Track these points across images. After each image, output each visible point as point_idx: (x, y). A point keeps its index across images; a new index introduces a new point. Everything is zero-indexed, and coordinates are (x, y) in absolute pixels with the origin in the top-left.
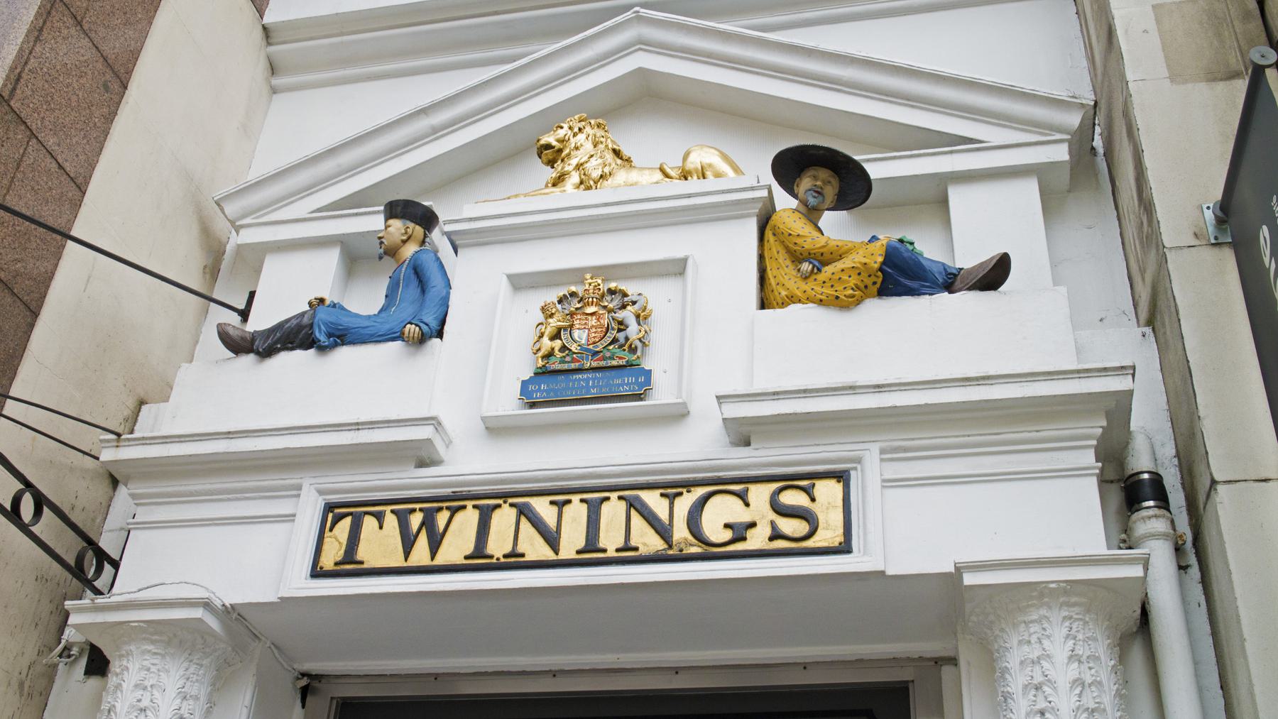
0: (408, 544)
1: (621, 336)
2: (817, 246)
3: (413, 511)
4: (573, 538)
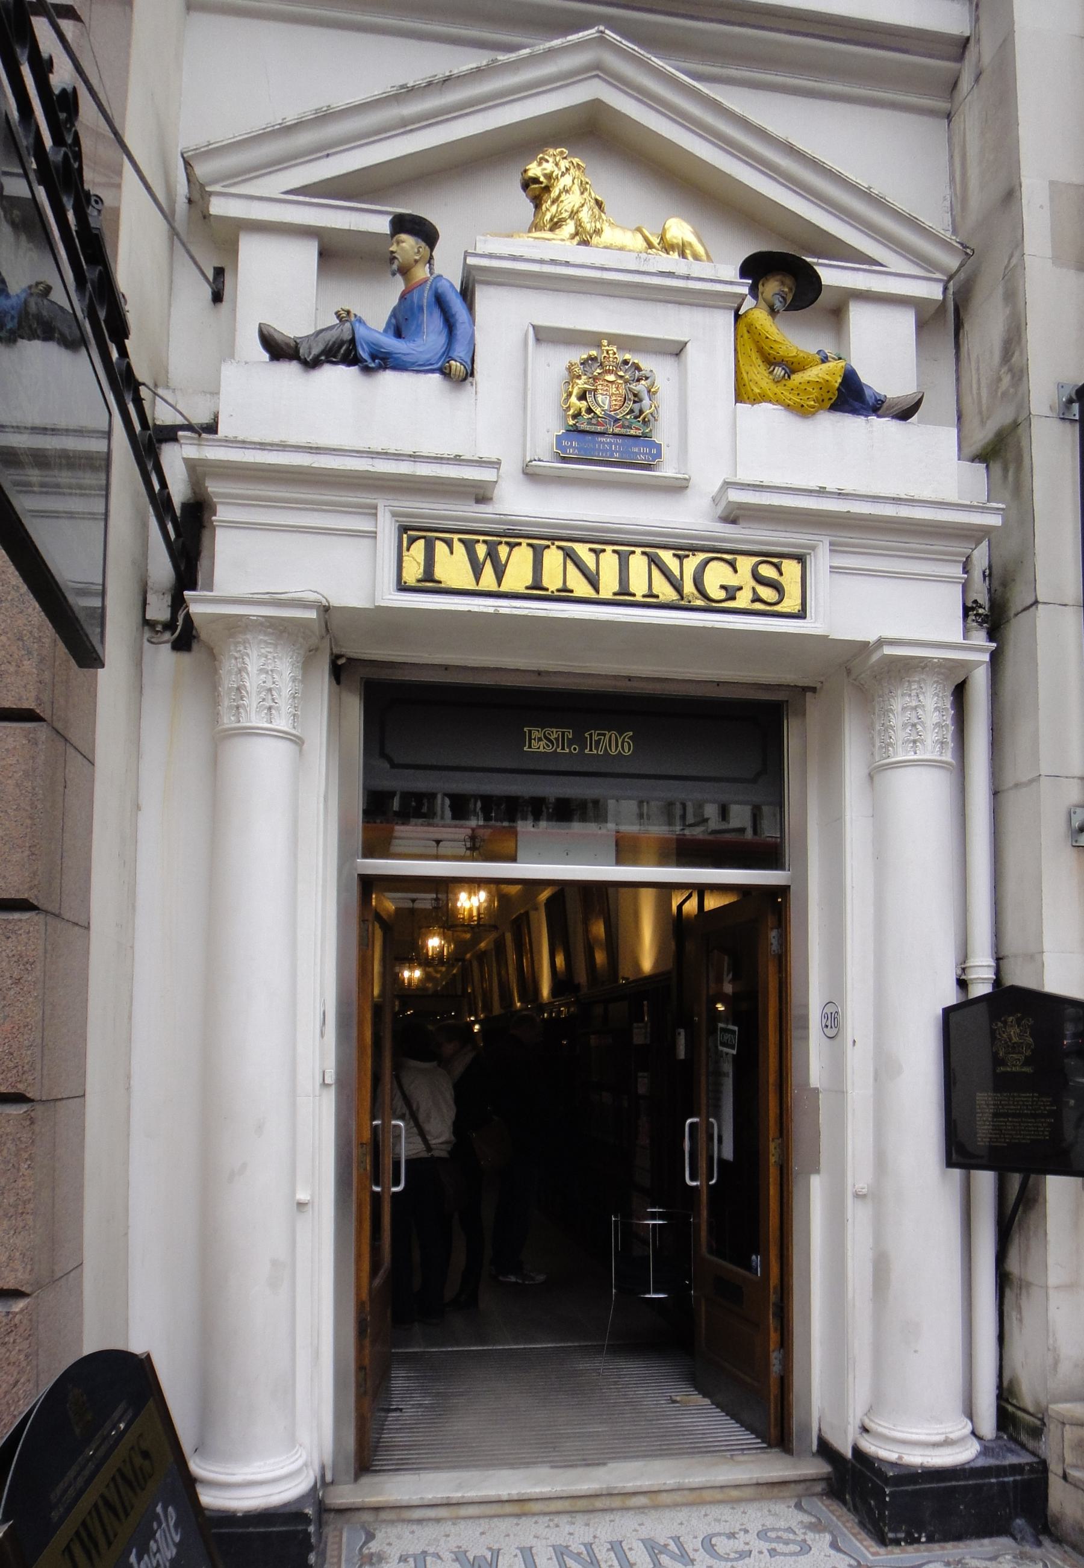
0: (477, 570)
2: (790, 355)
3: (478, 541)
4: (609, 585)
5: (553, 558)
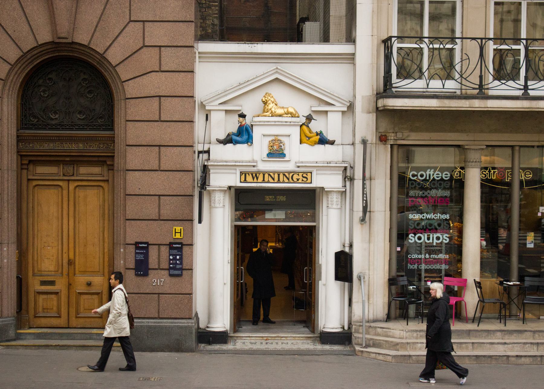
0: (253, 179)
1: (281, 148)
5: (266, 176)
